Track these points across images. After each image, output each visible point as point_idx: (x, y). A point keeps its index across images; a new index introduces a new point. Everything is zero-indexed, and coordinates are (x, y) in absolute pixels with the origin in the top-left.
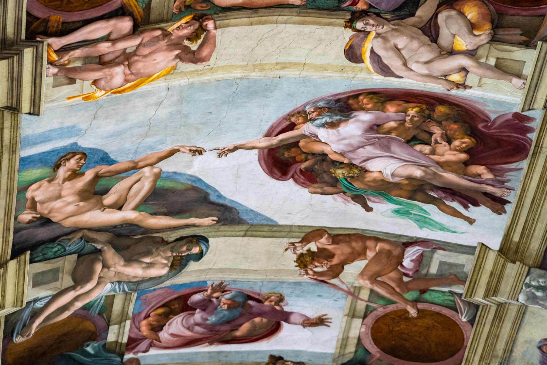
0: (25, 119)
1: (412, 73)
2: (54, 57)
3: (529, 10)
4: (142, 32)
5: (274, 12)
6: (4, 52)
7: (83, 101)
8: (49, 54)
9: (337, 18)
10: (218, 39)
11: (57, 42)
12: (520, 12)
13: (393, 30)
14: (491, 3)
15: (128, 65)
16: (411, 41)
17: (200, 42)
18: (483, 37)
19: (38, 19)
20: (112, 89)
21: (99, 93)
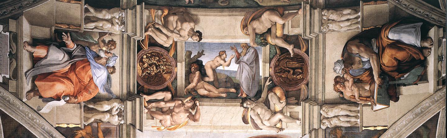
0: (137, 131)
1: (265, 126)
2: (146, 105)
3: (295, 88)
4: (175, 100)
5: (218, 101)
6: (130, 97)
7: (157, 130)
8: (144, 103)
9: (238, 102)
10: (201, 111)
11: (148, 98)
12: (292, 89)
13: (256, 105)
14: (283, 87)
15: (171, 115)
16: (262, 110)
17: (195, 110)
18: (284, 103)
19: (141, 85)
20: (167, 127)
21: (162, 128)
